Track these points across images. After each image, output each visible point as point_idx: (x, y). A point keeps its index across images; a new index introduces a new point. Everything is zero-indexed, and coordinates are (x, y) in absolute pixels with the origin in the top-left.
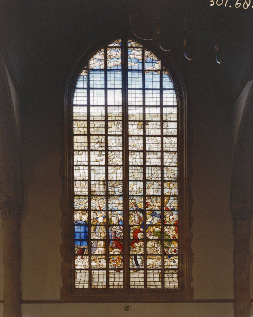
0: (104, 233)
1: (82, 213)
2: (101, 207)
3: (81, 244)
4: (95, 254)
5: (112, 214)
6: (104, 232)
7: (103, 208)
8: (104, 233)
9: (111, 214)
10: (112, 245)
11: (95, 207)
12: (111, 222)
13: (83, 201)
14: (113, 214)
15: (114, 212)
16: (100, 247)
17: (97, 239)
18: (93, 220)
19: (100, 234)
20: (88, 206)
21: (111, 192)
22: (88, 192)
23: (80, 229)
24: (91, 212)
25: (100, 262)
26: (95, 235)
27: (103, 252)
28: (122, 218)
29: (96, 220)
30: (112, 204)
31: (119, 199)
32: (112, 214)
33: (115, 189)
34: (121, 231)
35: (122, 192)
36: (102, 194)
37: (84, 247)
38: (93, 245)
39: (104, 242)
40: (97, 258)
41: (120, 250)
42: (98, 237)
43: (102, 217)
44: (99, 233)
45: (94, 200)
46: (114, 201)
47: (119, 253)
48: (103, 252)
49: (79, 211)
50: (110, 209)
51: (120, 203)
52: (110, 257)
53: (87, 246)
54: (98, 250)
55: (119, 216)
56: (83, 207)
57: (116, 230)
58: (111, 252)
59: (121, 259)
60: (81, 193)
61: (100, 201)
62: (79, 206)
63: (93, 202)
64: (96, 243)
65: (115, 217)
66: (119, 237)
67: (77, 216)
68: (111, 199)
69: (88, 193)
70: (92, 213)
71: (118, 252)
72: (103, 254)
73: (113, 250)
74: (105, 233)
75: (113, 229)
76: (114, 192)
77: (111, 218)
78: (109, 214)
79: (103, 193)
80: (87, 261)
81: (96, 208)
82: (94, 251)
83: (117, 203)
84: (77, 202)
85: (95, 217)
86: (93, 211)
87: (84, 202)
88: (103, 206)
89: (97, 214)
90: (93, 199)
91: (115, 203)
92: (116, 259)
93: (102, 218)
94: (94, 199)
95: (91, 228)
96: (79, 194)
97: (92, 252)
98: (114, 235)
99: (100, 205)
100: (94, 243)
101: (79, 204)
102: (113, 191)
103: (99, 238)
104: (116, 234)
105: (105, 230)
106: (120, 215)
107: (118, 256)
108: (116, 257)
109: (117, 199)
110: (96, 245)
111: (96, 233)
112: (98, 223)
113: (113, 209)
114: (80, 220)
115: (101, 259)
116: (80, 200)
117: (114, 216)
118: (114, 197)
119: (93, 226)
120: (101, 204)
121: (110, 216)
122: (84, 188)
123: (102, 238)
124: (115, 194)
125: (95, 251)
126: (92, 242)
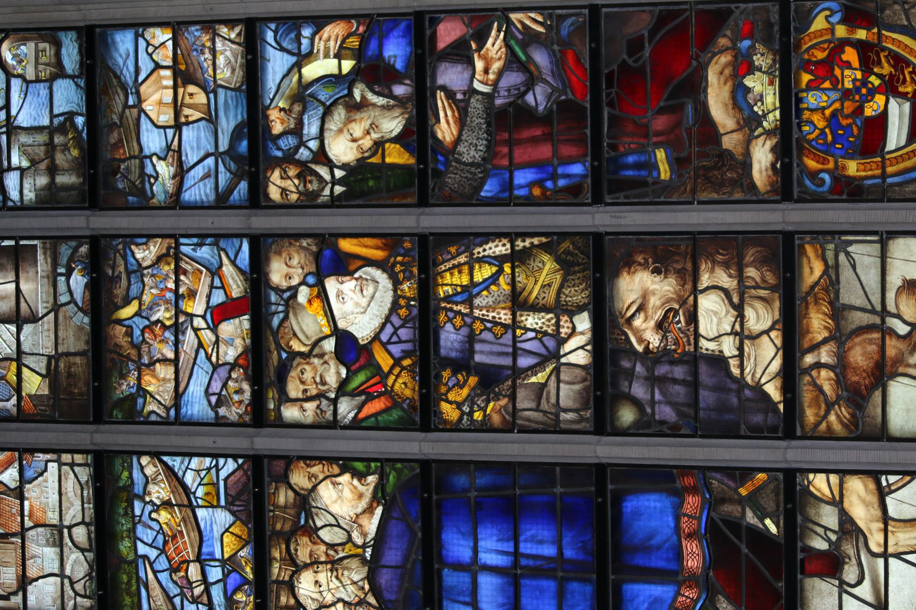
0: (518, 258)
1: (288, 537)
2: (218, 298)
3: (657, 562)
4: (773, 390)
5: (289, 158)
6: (500, 260)
7: (228, 269)
8: (518, 258)
9: (292, 172)
10: (661, 154)
11: (223, 372)
12: (383, 166)
13: (164, 516)
14: (288, 142)
15: (277, 128)
16: (693, 318)
17: (581, 358)
18: (370, 398)
19: (531, 320)
20: (208, 460)
21: (52, 170)
22: (66, 458)
23: (474, 568)
24: (281, 424)
25: (884, 312)
26: (539, 378)
27: (751, 272)
28: (334, 32)
29: (362, 361)
30: (191, 157)
31: (128, 76)
32: (289, 158)
33: (23, 120)
34: (495, 46)
35: (58, 45)
36: (78, 281)
37: (686, 525)
38: (666, 413)
39: (629, 264)
40: (825, 355)
41: (723, 42)
42: (562, 341)
43: (332, 285)
44: (515, 325)
45: (151, 385)
46: (152, 141)
47: (762, 60)
48: (751, 272)
49: (275, 569)
50: (243, 186)
51: (165, 56)
52: (814, 175)
53: (679, 495)
54: (728, 347)
55: (312, 71)
56: (223, 518)
57: (476, 105)
58: (747, 165)
59: (841, 31)
60: (80, 534)
61: (163, 314)
62: (215, 574)
63: (167, 397)
64: (639, 368)
65: (333, 125)
66: (559, 63)
67: (329, 598)
68: (134, 176)
69: (79, 458)
70: (291, 413)
71: (751, 69)
72: (771, 279)
73: (730, 142)
74: (520, 244)
75: (471, 152)
76: (58, 139)
77: (339, 174)
78: (294, 197)
79: (68, 275)
80: (874, 499)
81: (230, 354)
82: (734, 400)
83: (168, 96)
84: (174, 590)
85: (334, 373)
86: (271, 394)
87: (167, 504)
88: (205, 279)
89: (297, 346)
90: (142, 392)
91: (178, 126)
92: (834, 95)
93: (349, 285)
94: (132, 380)
95: (456, 428)
96: (91, 556)
97: (758, 419)
98: (538, 132)
99: (197, 307)
100: (639, 390)
101: (194, 571)
102: (41, 151)
103: (583, 322)
104: (530, 98)
105: (478, 251)
106: (303, 58)
107: (806, 78)
108: (812, 99)
109: (131, 102)
110: (662, 370)
111: (524, 362)
112: (404, 333)
113: (244, 146)
114: (373, 568)
115: (838, 312)
116: (153, 554)
117: (311, 128)
118: (114, 137)
119: (445, 407)
120: (192, 294)
121: (313, 187)
122: (19, 493)
123: (577, 294)
124: (80, 121)
125: (740, 381)
126: (627, 416)
